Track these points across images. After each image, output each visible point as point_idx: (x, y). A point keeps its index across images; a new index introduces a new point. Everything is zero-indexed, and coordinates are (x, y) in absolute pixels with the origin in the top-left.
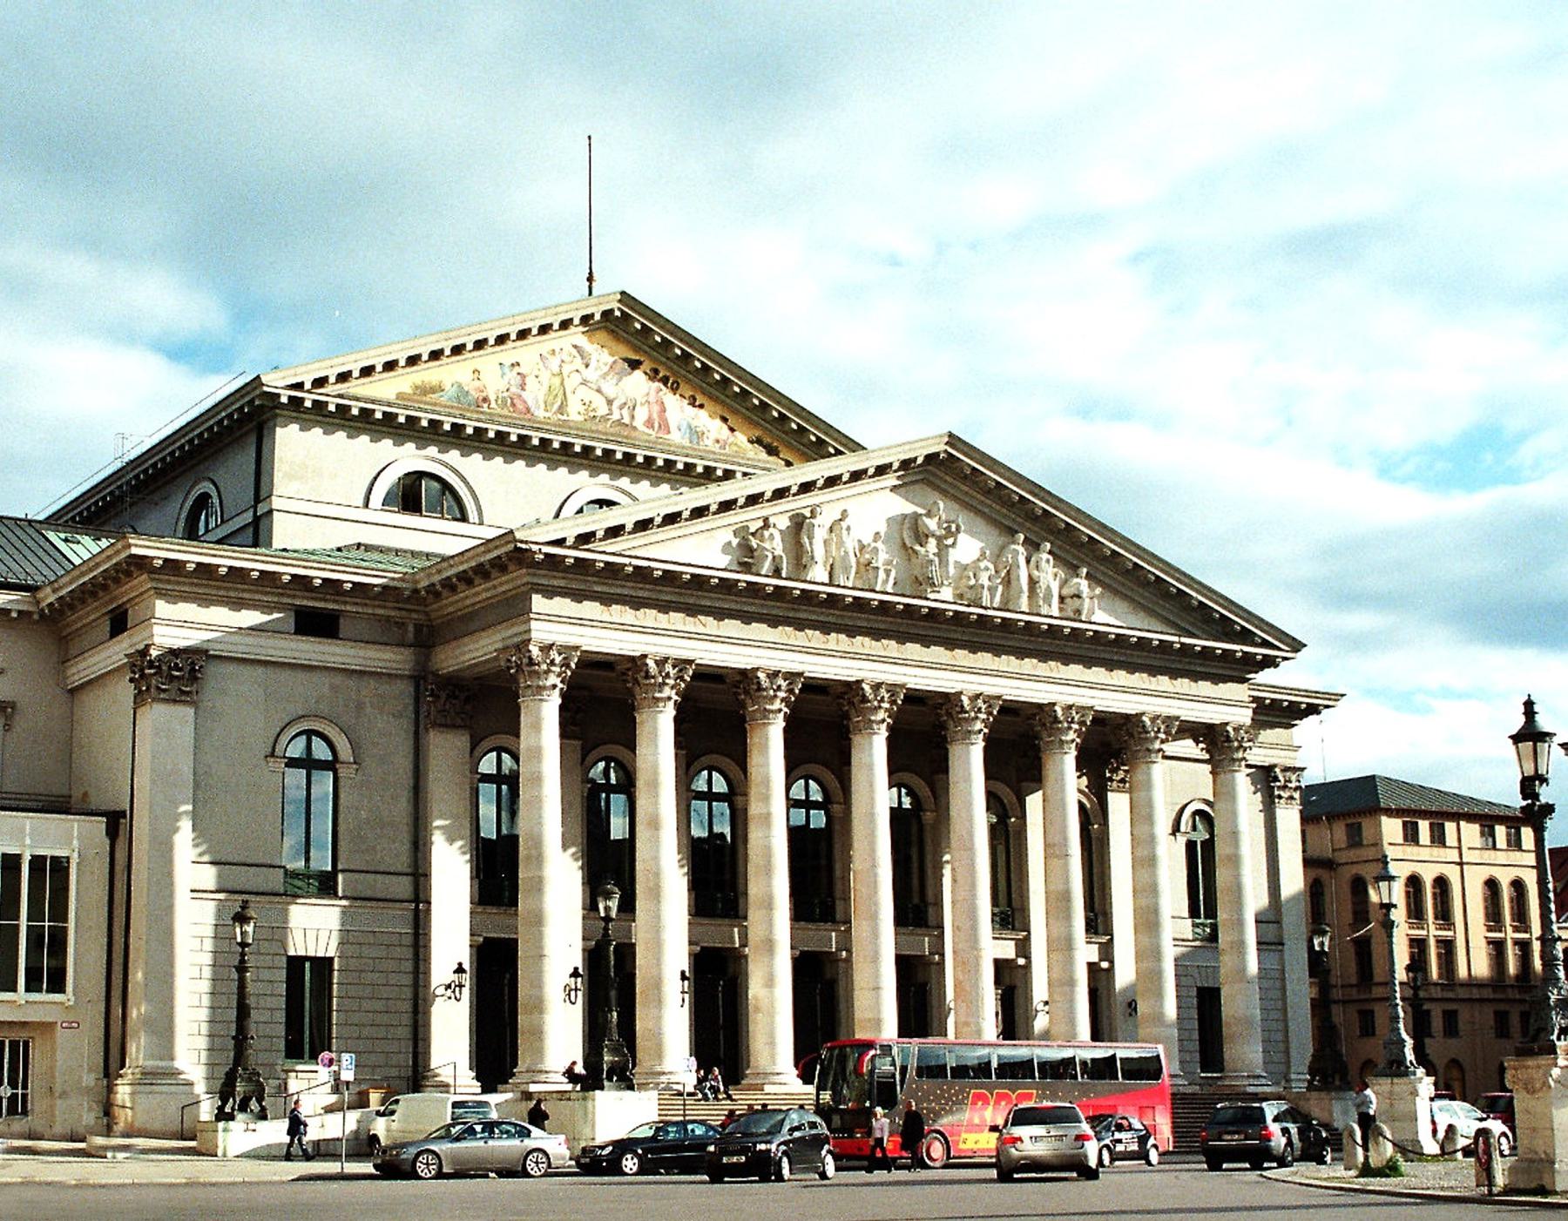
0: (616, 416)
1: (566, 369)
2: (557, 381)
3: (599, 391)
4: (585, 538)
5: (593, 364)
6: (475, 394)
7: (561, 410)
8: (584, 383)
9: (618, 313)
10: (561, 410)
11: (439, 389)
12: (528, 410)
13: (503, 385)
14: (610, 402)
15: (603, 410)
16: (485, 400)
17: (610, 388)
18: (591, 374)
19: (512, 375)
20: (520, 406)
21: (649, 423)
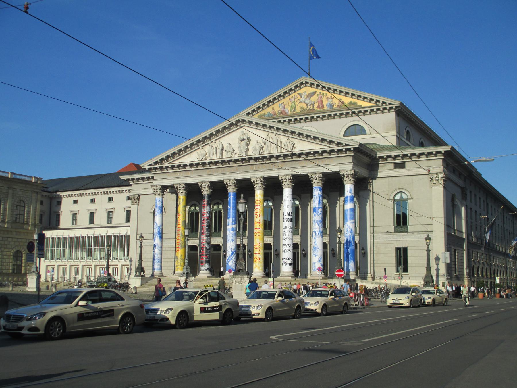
0: (309, 108)
1: (296, 100)
2: (293, 104)
3: (304, 103)
4: (156, 163)
5: (303, 96)
6: (273, 113)
7: (294, 111)
8: (301, 102)
9: (304, 82)
10: (294, 111)
11: (265, 114)
12: (286, 113)
13: (279, 109)
14: (307, 105)
15: (305, 106)
16: (275, 114)
17: (307, 101)
18: (302, 99)
19: (282, 106)
20: (284, 113)
21: (318, 107)
